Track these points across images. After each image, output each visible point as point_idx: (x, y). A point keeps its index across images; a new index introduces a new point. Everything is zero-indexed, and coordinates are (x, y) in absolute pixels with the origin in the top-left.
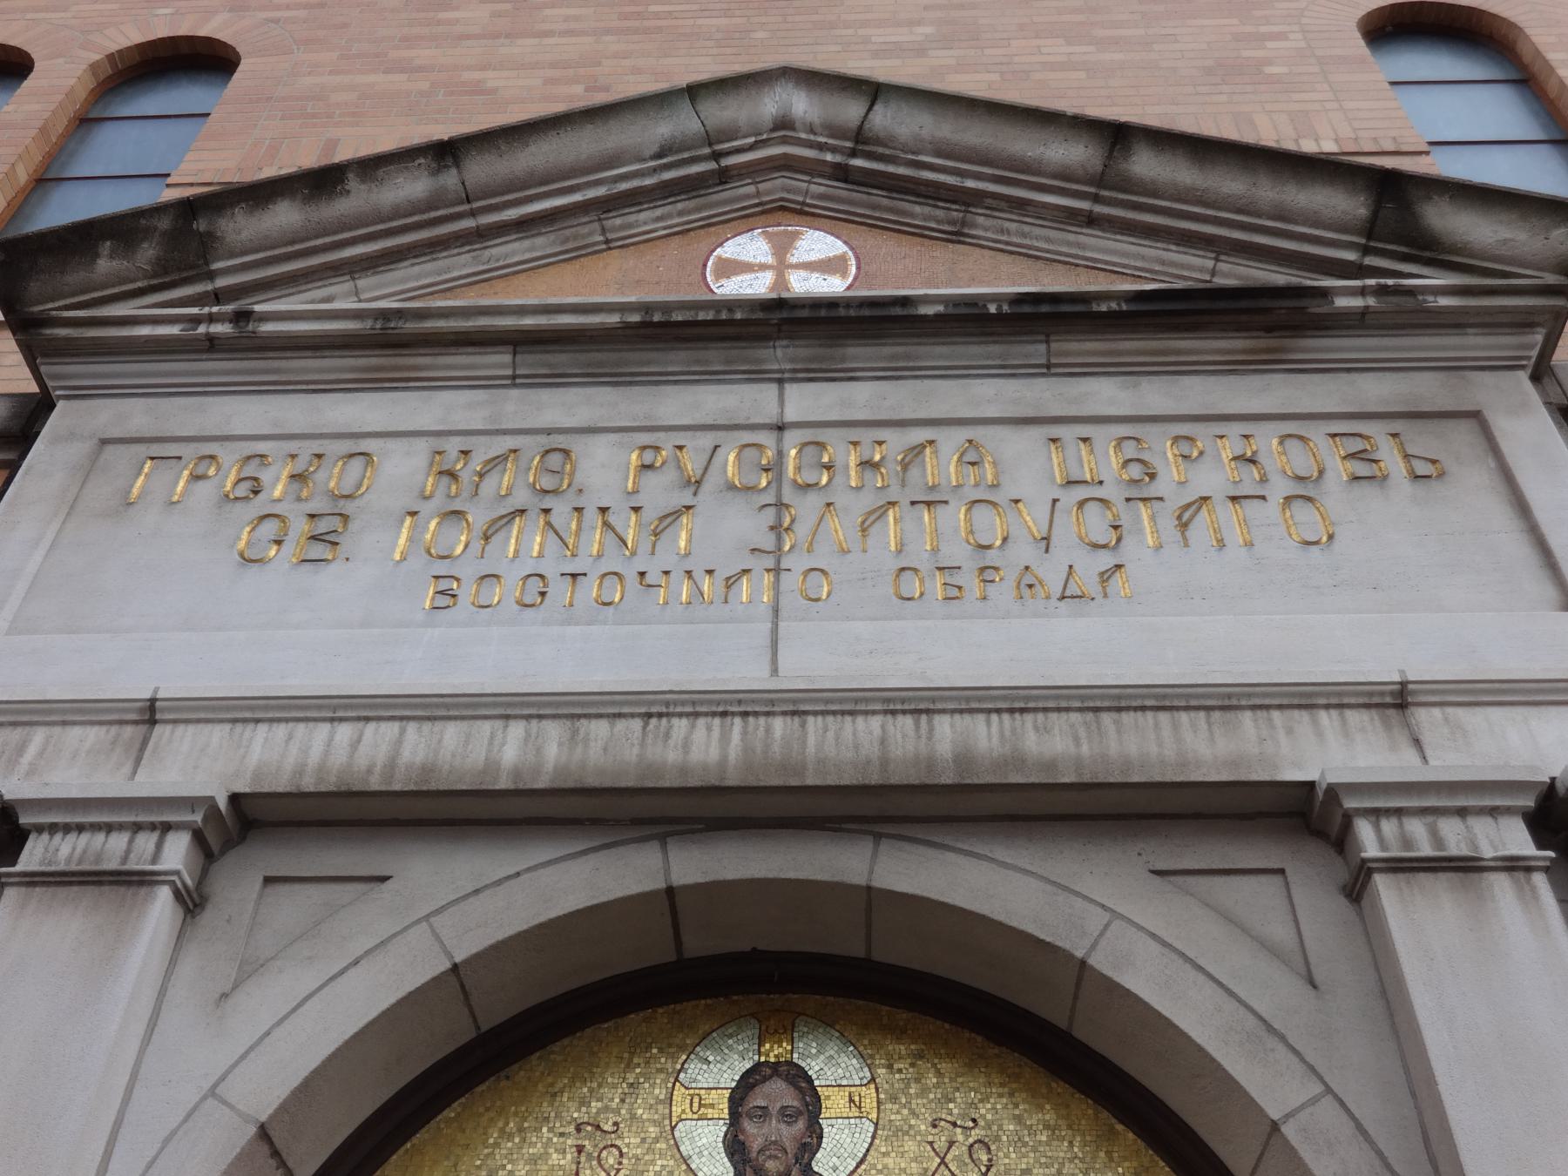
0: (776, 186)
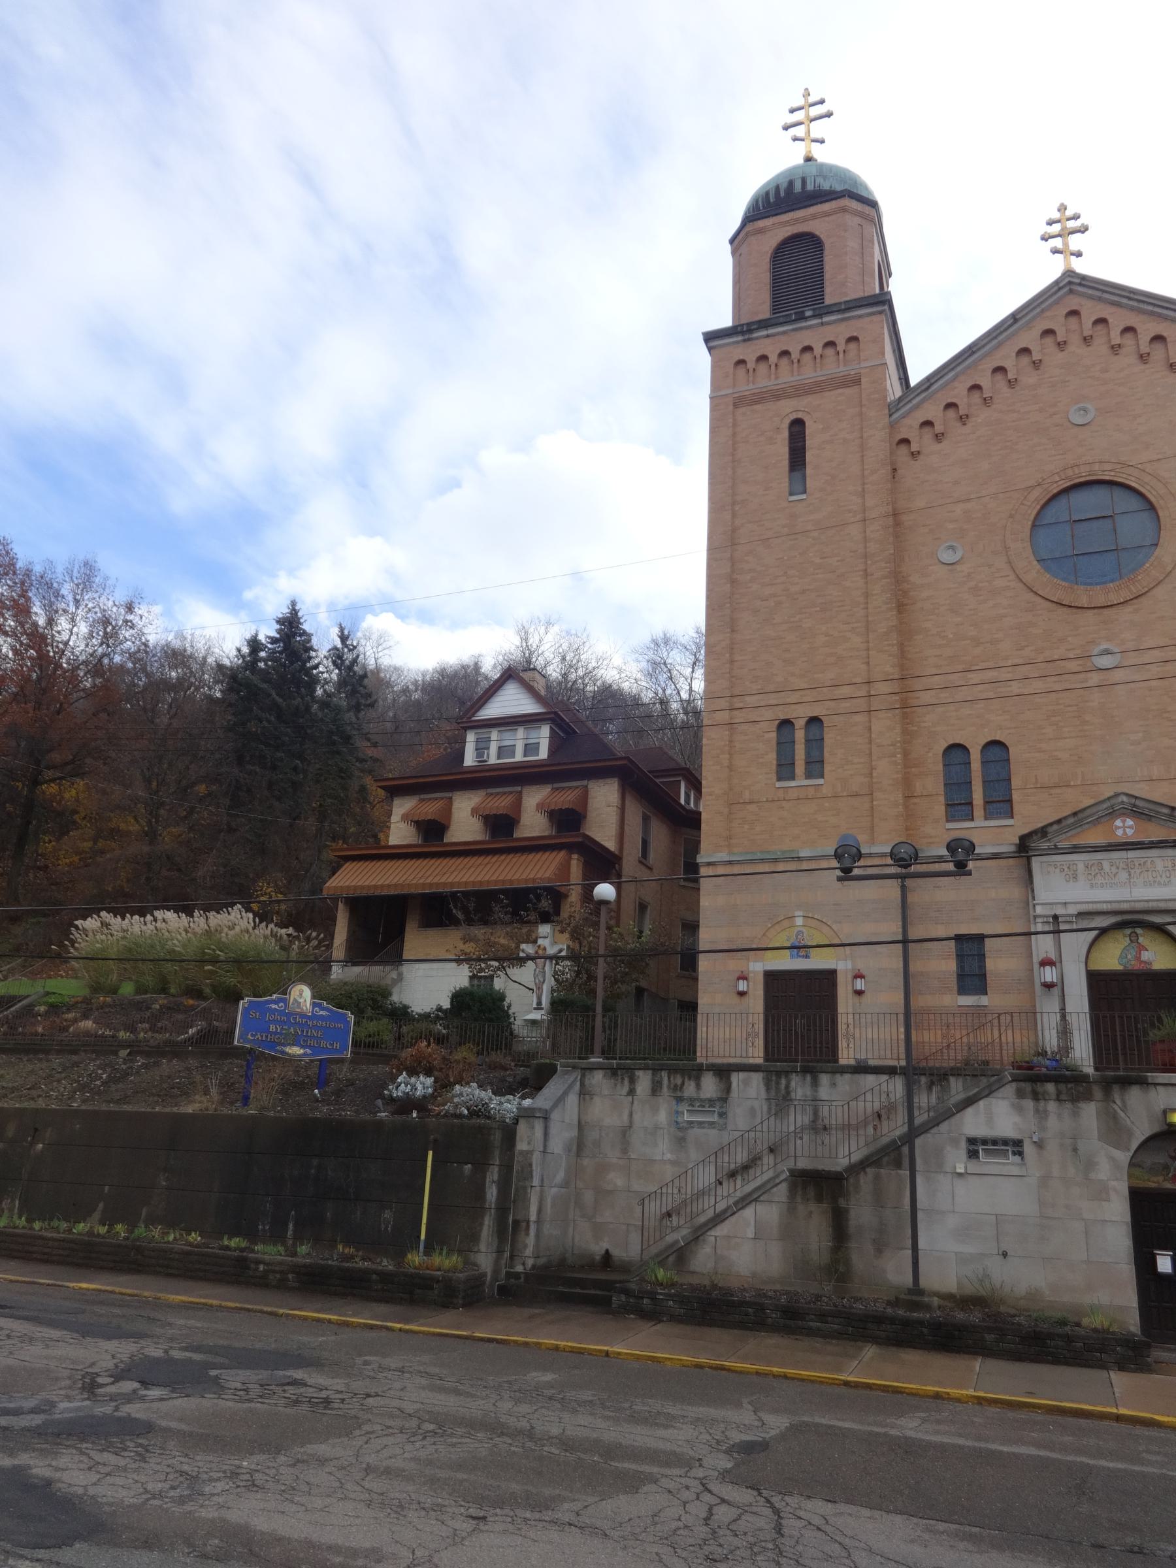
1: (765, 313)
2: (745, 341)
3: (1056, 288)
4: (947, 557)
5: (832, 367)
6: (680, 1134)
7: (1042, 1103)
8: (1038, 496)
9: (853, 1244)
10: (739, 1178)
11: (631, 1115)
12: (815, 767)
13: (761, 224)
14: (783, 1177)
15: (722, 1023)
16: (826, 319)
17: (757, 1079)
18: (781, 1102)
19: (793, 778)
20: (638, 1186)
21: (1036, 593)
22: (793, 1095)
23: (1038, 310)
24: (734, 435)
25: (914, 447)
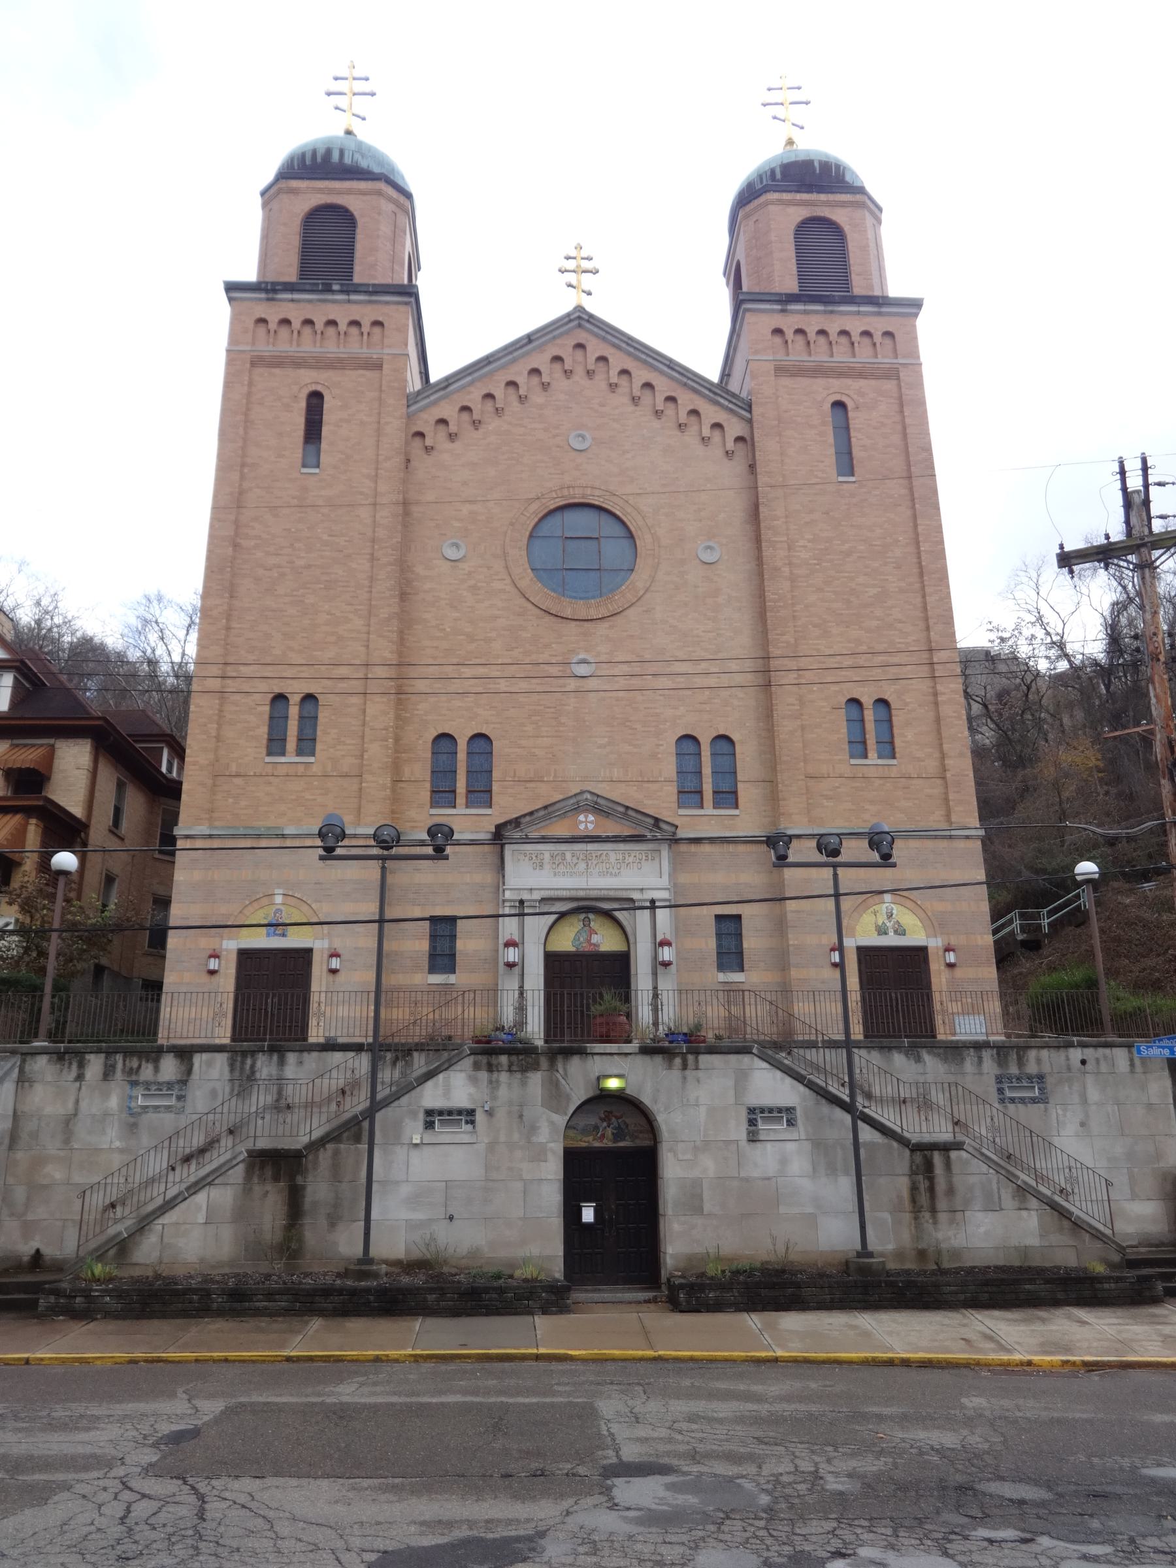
0: (585, 807)
1: (291, 274)
2: (268, 299)
3: (567, 319)
4: (451, 553)
5: (354, 347)
6: (132, 1120)
7: (495, 1075)
8: (535, 510)
9: (307, 1221)
10: (194, 1162)
11: (77, 1102)
12: (307, 744)
13: (295, 184)
14: (241, 1158)
15: (188, 1003)
16: (353, 297)
17: (221, 1059)
18: (244, 1082)
19: (283, 754)
20: (79, 1178)
21: (528, 599)
22: (258, 1075)
23: (550, 336)
24: (249, 394)
25: (429, 442)
